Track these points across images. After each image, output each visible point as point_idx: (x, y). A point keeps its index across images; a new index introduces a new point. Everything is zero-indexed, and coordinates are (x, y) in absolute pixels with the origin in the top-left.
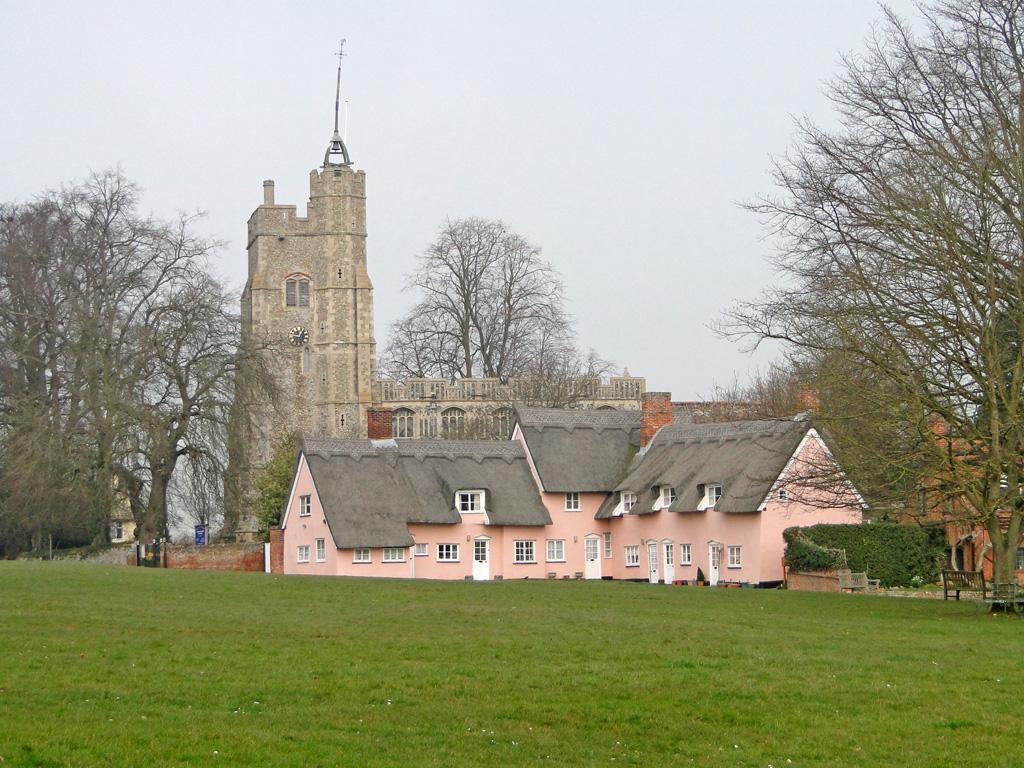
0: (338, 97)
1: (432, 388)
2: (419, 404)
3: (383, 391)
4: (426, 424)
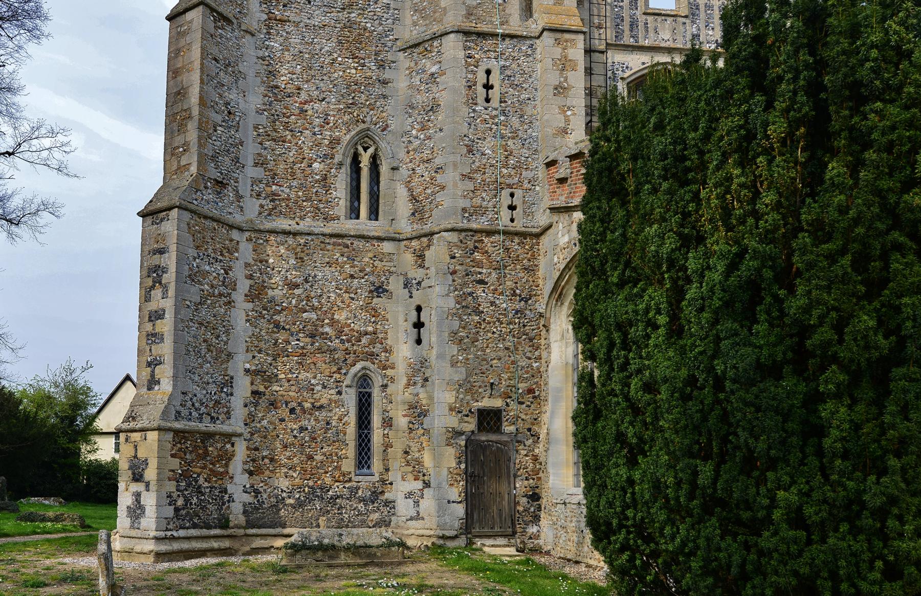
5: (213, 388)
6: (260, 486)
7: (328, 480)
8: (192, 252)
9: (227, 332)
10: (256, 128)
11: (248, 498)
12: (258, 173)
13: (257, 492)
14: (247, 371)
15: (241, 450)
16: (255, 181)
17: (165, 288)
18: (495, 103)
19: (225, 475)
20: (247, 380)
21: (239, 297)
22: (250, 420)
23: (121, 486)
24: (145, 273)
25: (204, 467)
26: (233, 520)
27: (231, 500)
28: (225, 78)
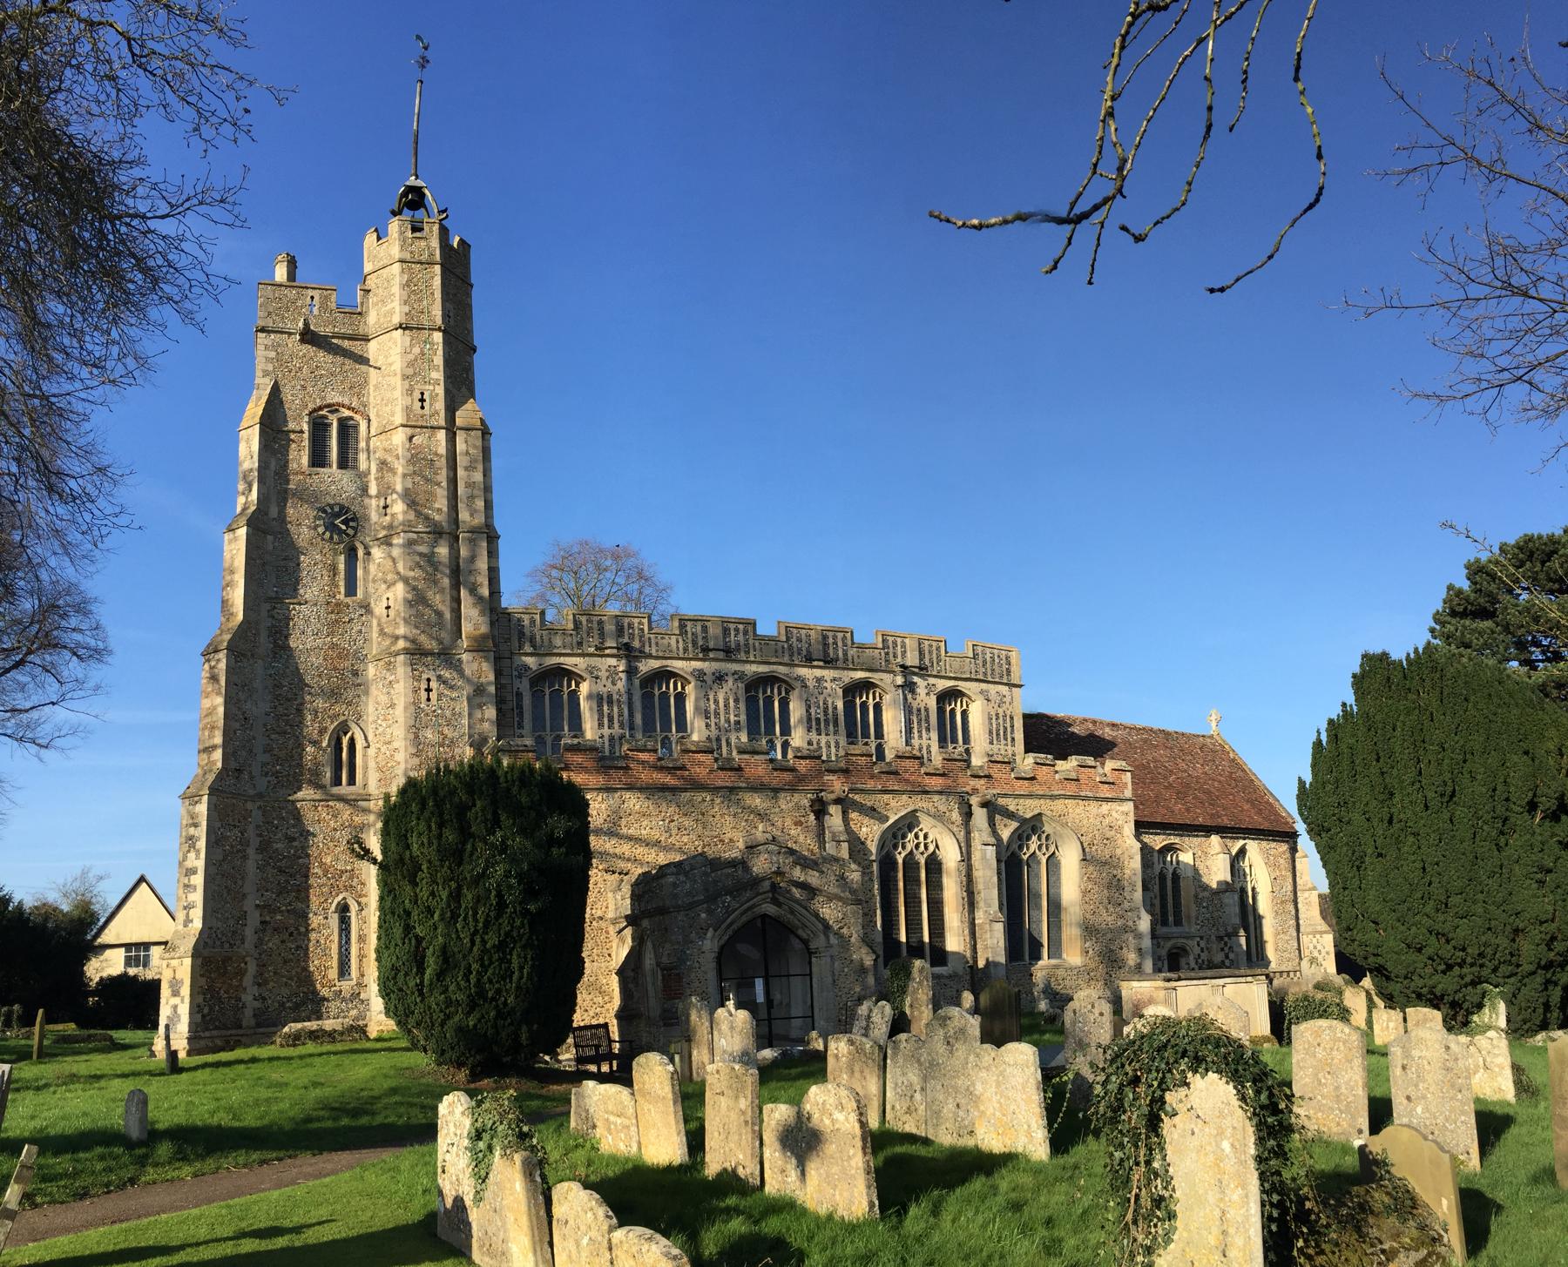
5: (232, 922)
6: (266, 994)
8: (218, 824)
9: (243, 878)
10: (265, 725)
11: (257, 1004)
12: (266, 758)
13: (264, 999)
14: (257, 906)
16: (264, 764)
17: (198, 852)
19: (241, 988)
20: (257, 914)
21: (251, 851)
23: (163, 1001)
24: (183, 840)
25: (224, 983)
26: (244, 1024)
27: (244, 1006)
28: (242, 696)
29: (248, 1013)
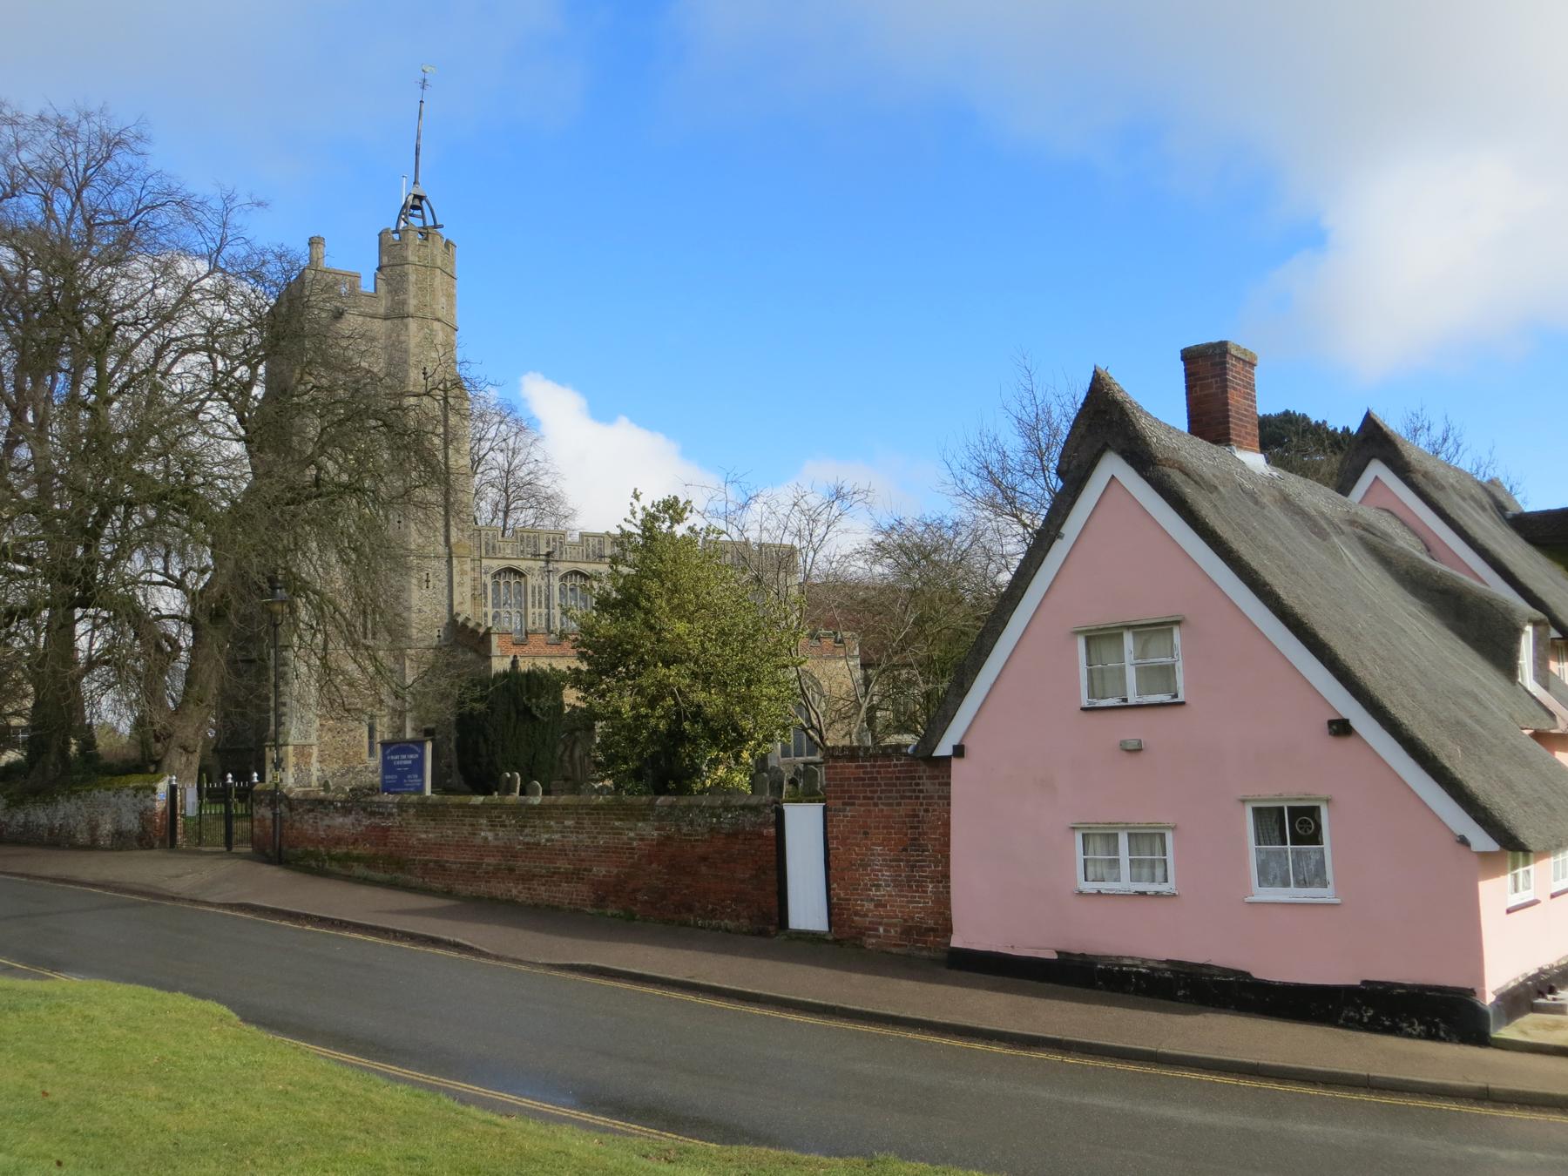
0: (418, 138)
1: (548, 543)
2: (531, 563)
3: (483, 543)
4: (540, 592)
6: (325, 768)
7: (355, 763)
15: (315, 751)
18: (431, 587)
22: (320, 737)
26: (313, 784)
29: (314, 778)
